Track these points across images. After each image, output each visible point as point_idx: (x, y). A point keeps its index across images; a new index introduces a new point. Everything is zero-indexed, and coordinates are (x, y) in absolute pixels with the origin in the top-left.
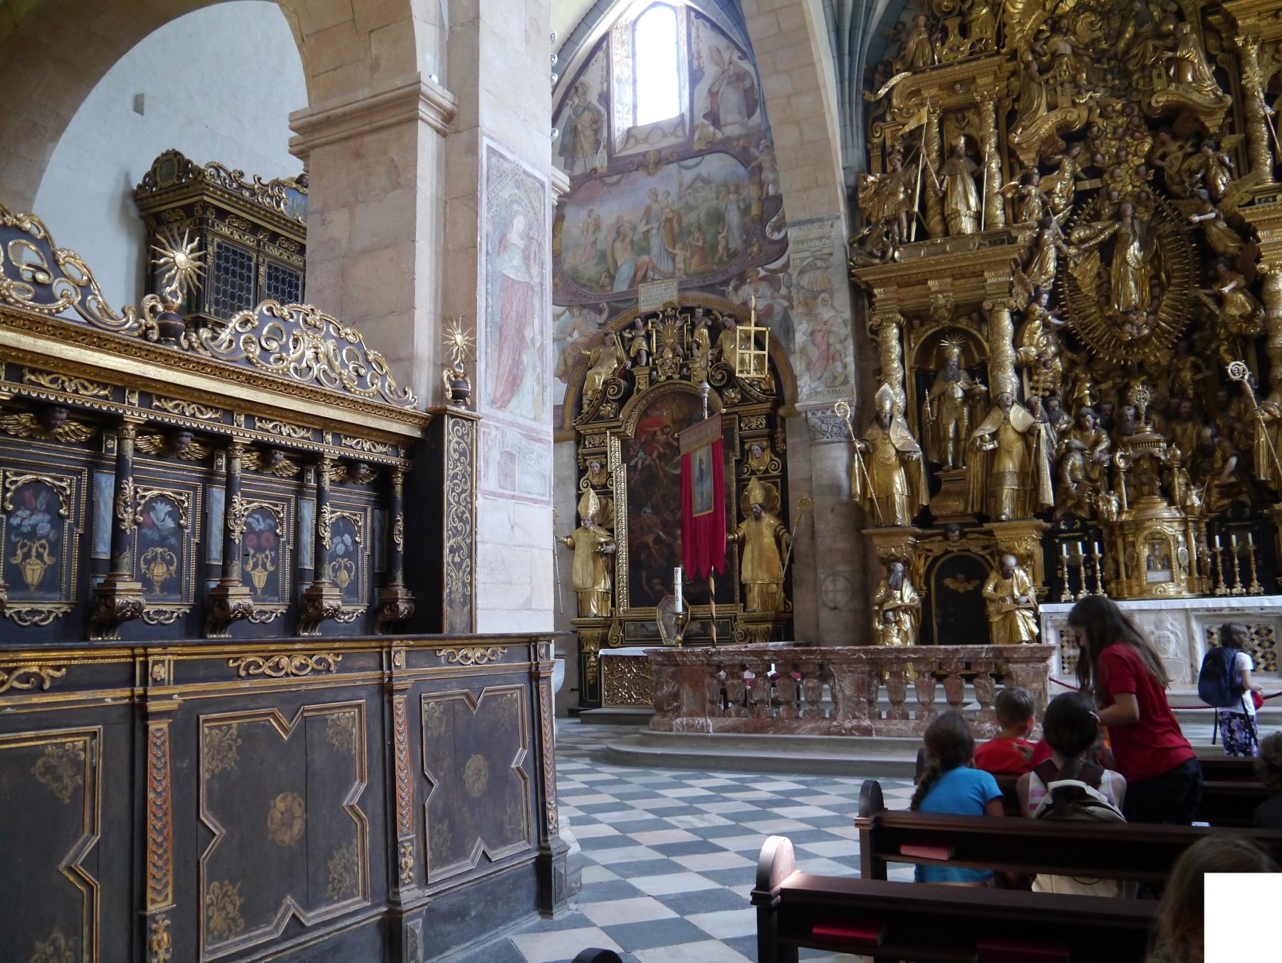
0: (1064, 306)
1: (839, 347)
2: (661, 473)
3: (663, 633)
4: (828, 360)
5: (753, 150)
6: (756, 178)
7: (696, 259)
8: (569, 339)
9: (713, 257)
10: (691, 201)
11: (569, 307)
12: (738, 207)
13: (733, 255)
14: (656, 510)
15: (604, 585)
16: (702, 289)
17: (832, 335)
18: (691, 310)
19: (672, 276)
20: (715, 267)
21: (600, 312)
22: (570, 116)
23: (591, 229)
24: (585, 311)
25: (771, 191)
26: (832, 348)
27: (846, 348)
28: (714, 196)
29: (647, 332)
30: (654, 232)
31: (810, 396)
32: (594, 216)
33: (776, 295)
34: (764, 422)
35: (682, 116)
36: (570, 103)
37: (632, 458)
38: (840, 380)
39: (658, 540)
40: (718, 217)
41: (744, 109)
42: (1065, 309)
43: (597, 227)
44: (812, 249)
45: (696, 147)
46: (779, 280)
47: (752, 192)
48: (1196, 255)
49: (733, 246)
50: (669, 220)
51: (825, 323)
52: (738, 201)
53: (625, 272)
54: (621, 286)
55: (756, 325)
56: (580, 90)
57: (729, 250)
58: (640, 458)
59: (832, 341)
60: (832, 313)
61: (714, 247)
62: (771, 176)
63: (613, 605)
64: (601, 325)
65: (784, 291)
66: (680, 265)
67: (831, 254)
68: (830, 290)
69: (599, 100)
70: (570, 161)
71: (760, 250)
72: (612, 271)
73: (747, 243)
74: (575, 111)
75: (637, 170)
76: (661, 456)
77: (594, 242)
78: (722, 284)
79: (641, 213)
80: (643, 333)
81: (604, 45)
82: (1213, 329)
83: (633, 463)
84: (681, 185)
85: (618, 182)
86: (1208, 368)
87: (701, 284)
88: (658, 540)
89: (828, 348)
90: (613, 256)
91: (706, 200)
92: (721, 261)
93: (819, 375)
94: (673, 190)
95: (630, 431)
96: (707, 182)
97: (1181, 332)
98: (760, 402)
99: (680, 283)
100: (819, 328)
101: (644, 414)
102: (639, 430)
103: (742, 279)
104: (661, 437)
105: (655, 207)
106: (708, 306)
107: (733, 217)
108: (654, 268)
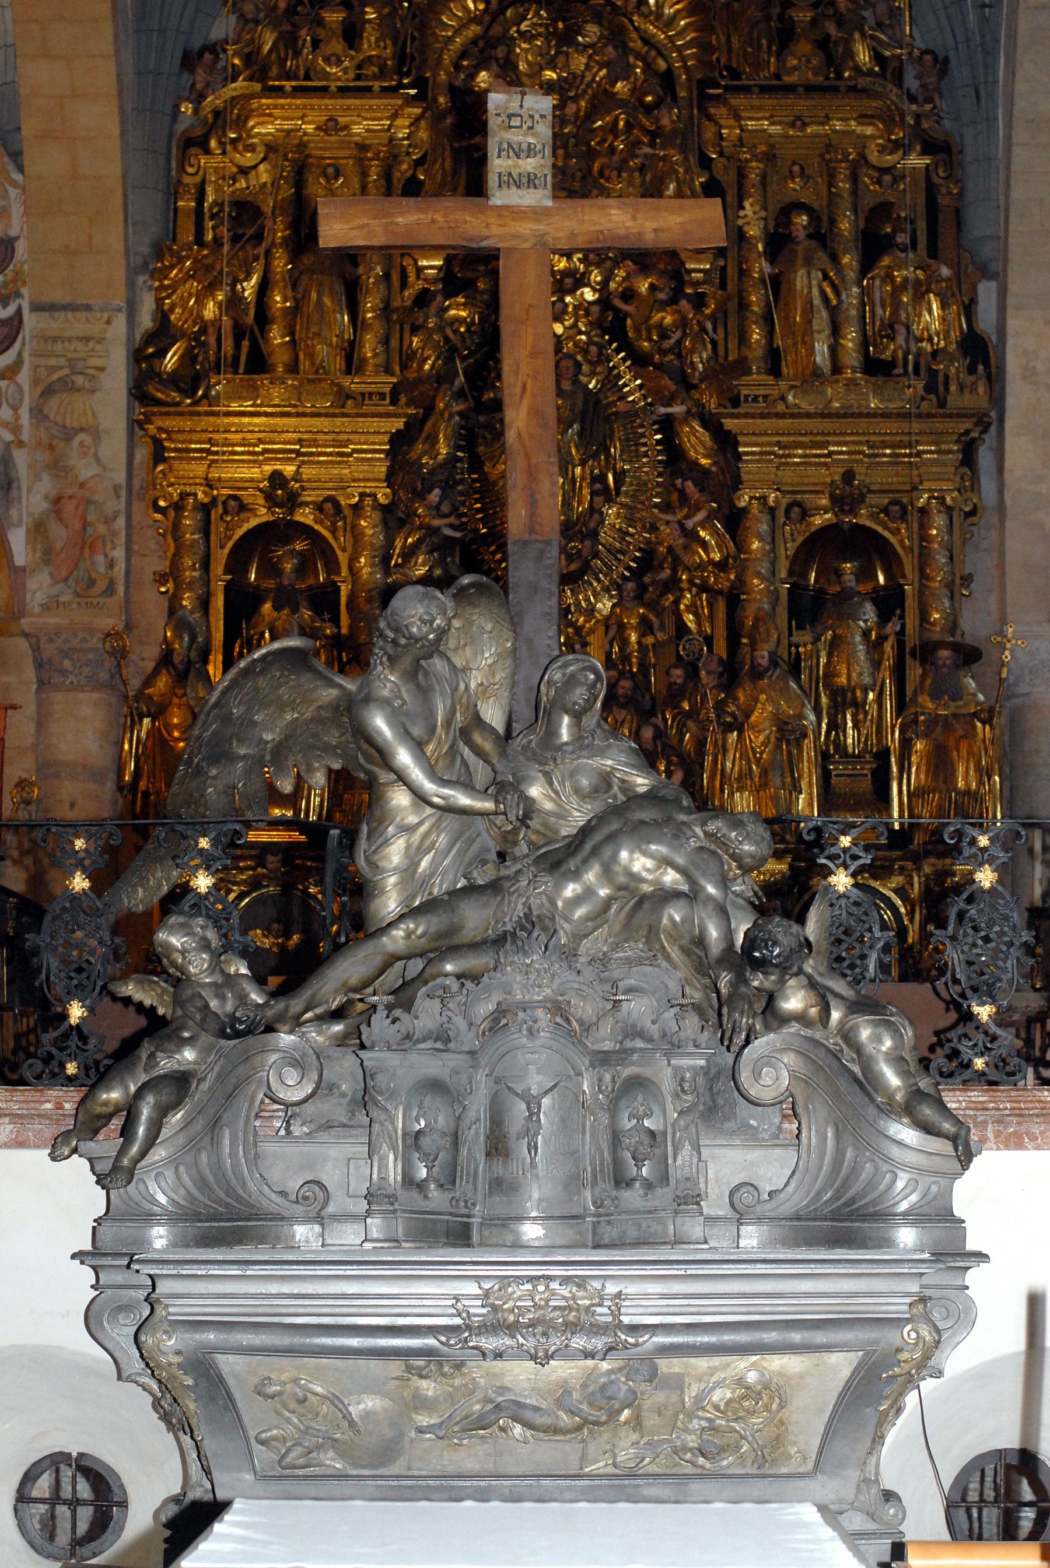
0: (465, 515)
1: (102, 529)
4: (83, 548)
17: (92, 507)
26: (90, 531)
27: (114, 534)
31: (45, 608)
38: (100, 586)
42: (464, 520)
44: (70, 355)
48: (659, 452)
51: (82, 485)
59: (91, 517)
60: (94, 470)
67: (102, 369)
68: (95, 431)
82: (674, 571)
86: (662, 628)
89: (84, 529)
93: (64, 574)
97: (629, 568)
100: (69, 492)
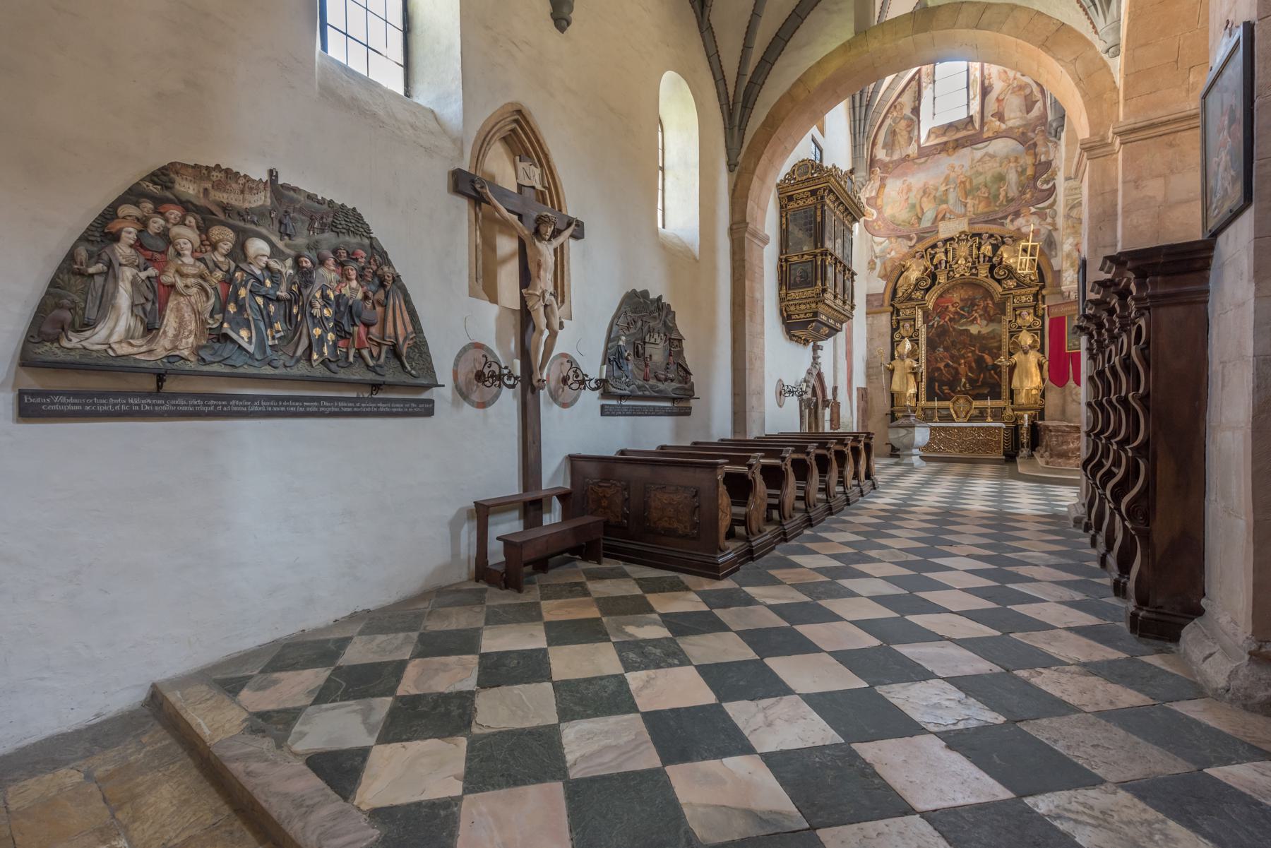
2: (951, 329)
3: (954, 415)
5: (1031, 134)
6: (1032, 151)
7: (982, 204)
8: (888, 256)
9: (996, 202)
10: (980, 169)
11: (889, 237)
12: (1017, 171)
13: (1010, 201)
14: (946, 349)
15: (912, 390)
16: (986, 222)
18: (980, 235)
19: (964, 215)
20: (997, 209)
21: (911, 239)
22: (890, 124)
23: (905, 191)
24: (900, 239)
25: (1043, 158)
28: (998, 165)
29: (946, 249)
30: (952, 190)
32: (907, 183)
33: (1042, 223)
34: (1032, 299)
35: (971, 118)
36: (891, 116)
37: (931, 321)
39: (947, 365)
40: (1000, 178)
41: (1024, 108)
43: (909, 190)
45: (985, 136)
46: (1046, 214)
47: (1029, 160)
49: (1011, 195)
50: (963, 182)
52: (1016, 167)
53: (929, 215)
54: (926, 223)
55: (1032, 242)
56: (898, 107)
57: (1007, 197)
58: (936, 321)
61: (997, 196)
62: (1044, 149)
63: (917, 400)
64: (910, 247)
65: (1049, 220)
66: (970, 208)
69: (912, 112)
70: (890, 151)
71: (1032, 196)
72: (920, 215)
73: (1023, 193)
74: (894, 121)
75: (939, 153)
76: (951, 320)
77: (907, 199)
78: (1001, 218)
79: (942, 179)
80: (943, 250)
81: (917, 77)
83: (931, 324)
84: (973, 160)
85: (926, 161)
87: (986, 219)
88: (947, 365)
90: (921, 207)
91: (991, 168)
92: (1001, 205)
94: (967, 163)
95: (930, 306)
96: (992, 156)
98: (1030, 287)
99: (970, 220)
101: (941, 296)
102: (936, 305)
103: (1017, 214)
104: (952, 309)
105: (953, 175)
106: (991, 232)
107: (1012, 177)
108: (951, 212)
